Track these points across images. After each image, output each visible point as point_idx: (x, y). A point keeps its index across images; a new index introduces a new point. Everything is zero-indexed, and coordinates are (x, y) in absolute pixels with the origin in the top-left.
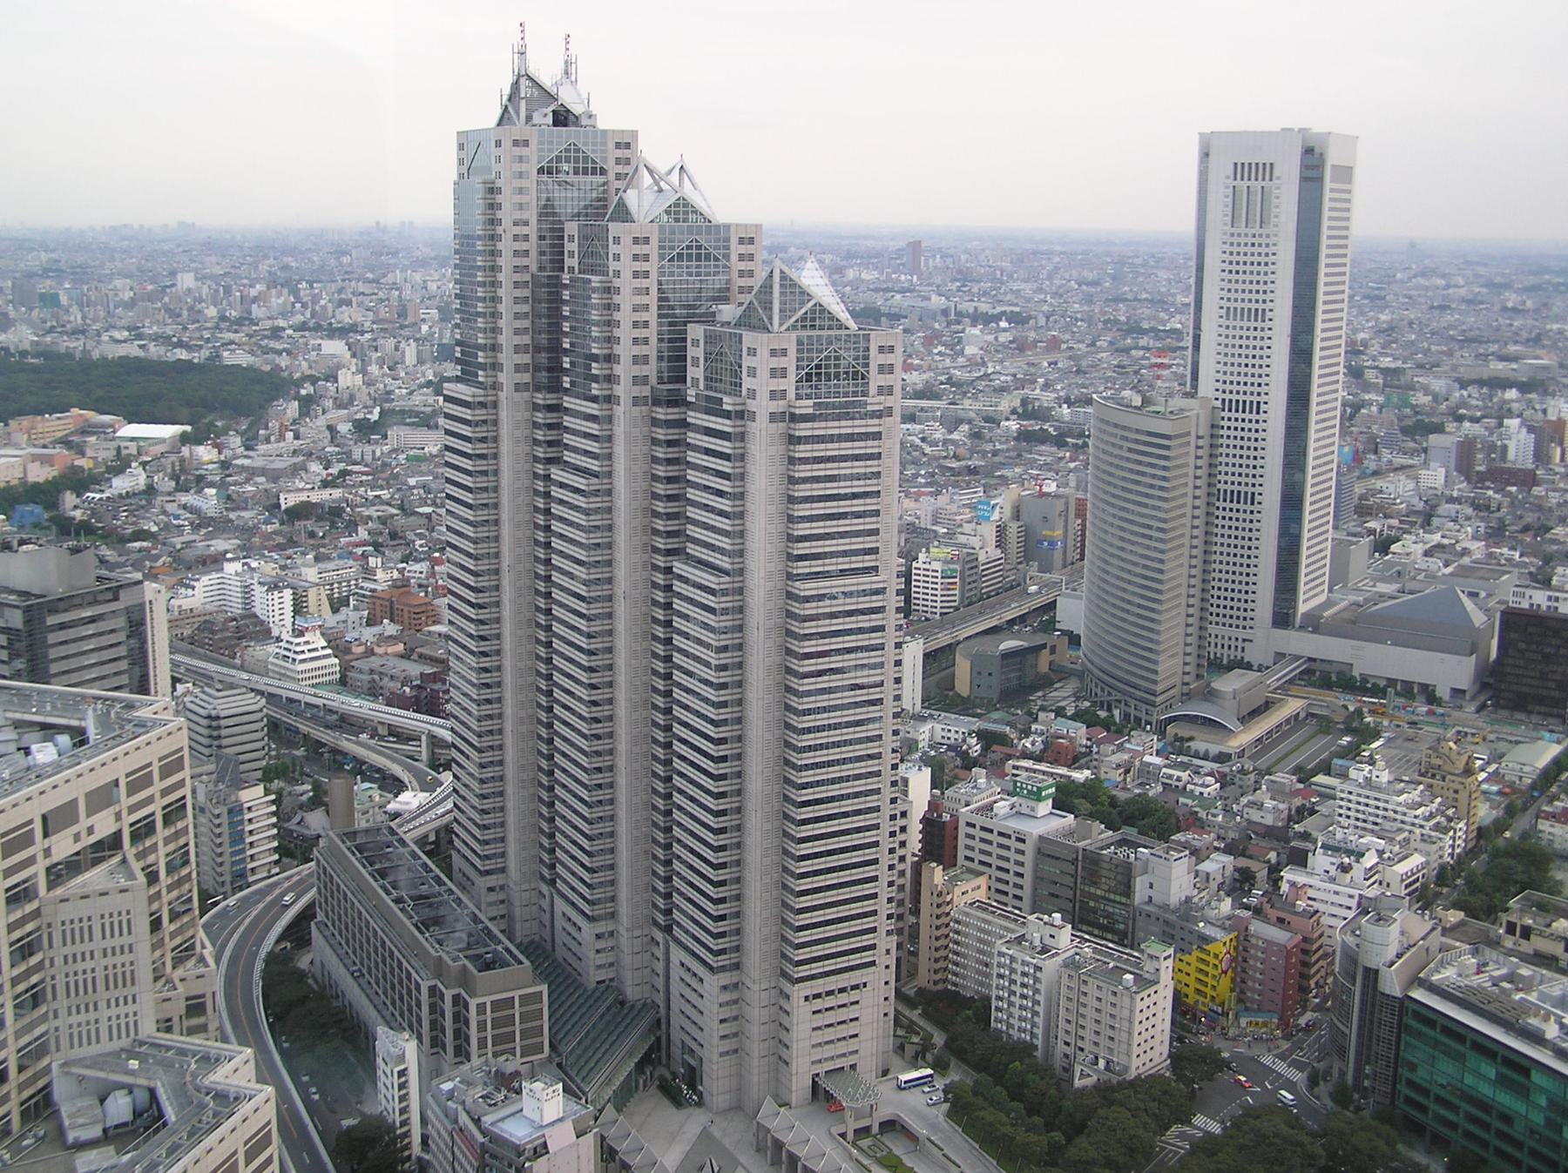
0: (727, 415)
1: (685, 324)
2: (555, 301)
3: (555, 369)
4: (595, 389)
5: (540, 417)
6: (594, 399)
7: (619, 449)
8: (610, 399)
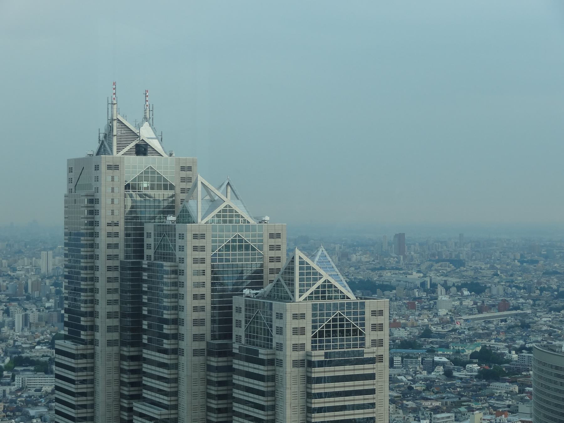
0: (261, 362)
1: (231, 296)
2: (137, 281)
3: (137, 330)
4: (167, 344)
5: (126, 365)
6: (165, 351)
7: (184, 388)
8: (176, 352)
